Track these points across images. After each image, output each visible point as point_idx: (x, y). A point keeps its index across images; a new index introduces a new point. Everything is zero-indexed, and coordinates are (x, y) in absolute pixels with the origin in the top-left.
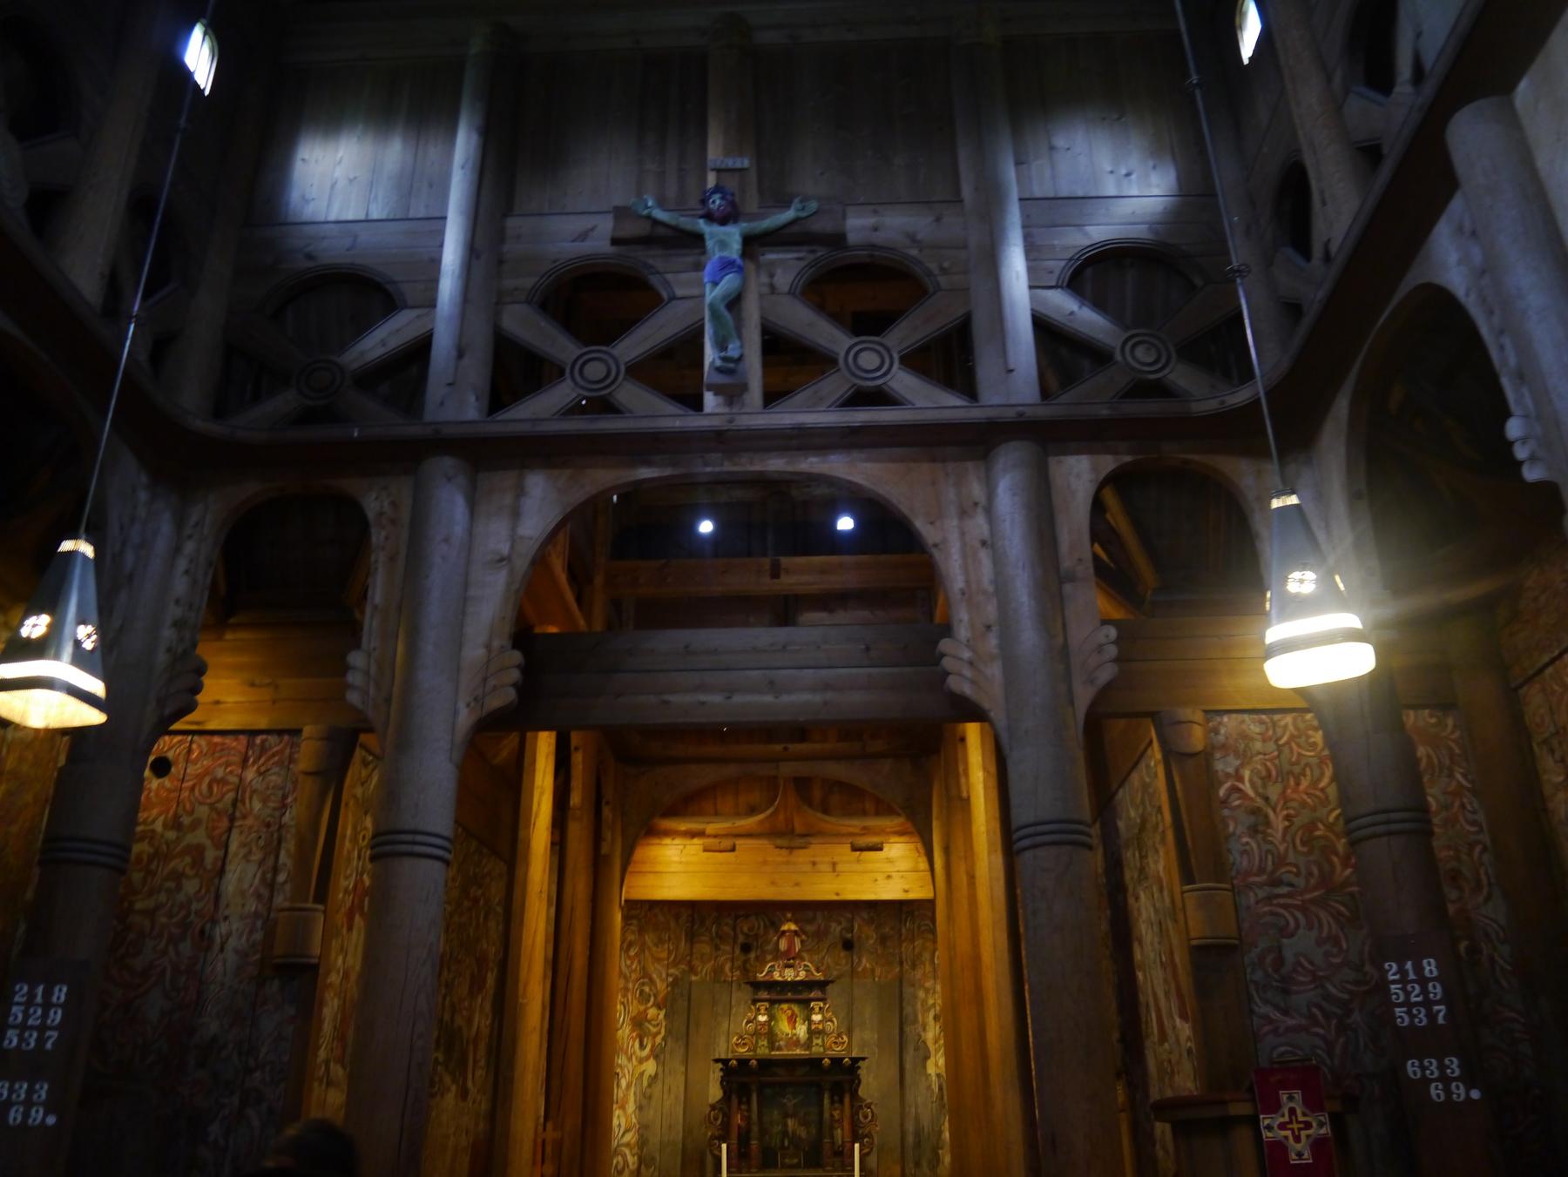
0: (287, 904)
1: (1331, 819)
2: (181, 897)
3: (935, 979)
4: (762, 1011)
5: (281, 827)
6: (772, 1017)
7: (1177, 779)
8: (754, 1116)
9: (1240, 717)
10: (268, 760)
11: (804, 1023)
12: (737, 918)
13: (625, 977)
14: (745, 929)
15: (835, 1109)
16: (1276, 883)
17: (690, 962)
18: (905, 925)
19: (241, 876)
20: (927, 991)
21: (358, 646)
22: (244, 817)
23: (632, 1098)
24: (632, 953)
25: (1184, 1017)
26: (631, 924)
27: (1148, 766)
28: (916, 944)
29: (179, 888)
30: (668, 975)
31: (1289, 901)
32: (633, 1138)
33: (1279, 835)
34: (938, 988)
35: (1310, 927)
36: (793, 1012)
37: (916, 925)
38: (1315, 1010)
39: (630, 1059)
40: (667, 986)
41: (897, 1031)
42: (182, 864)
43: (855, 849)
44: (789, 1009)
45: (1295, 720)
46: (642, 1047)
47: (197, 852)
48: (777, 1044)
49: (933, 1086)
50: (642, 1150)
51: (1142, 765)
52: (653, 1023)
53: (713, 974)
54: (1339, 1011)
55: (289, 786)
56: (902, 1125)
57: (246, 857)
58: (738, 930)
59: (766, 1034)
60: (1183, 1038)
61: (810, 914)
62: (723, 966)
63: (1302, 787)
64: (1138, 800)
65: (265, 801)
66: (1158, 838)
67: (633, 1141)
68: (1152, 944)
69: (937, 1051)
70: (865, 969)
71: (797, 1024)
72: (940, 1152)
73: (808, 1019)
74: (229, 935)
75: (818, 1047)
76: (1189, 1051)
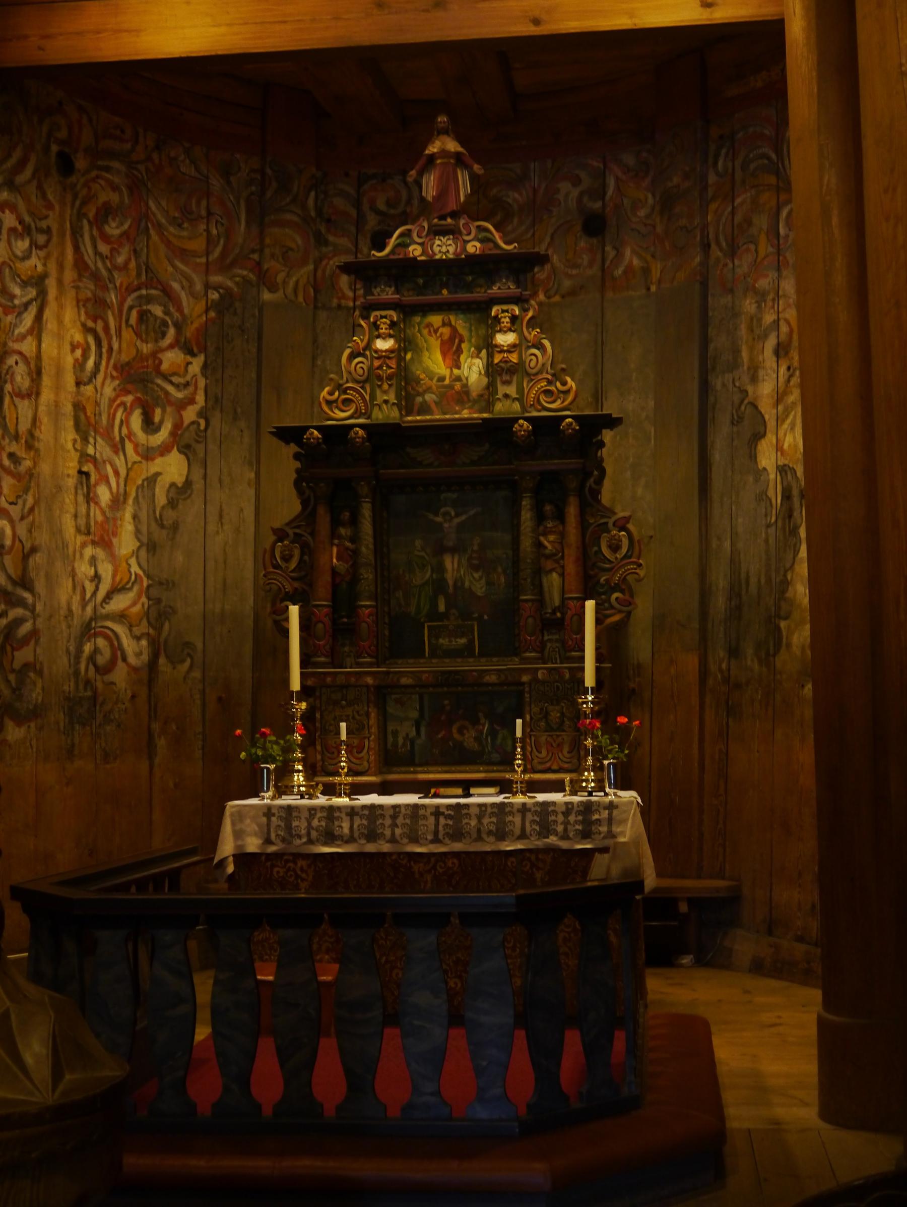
3: (779, 270)
4: (384, 330)
6: (406, 344)
11: (478, 357)
13: (96, 277)
14: (381, 206)
15: (545, 534)
17: (259, 264)
18: (715, 164)
20: (761, 296)
23: (128, 527)
24: (113, 229)
26: (108, 169)
28: (738, 201)
30: (207, 286)
32: (134, 604)
34: (788, 286)
36: (454, 330)
37: (738, 163)
39: (118, 447)
40: (207, 311)
41: (694, 387)
44: (444, 325)
46: (150, 425)
48: (419, 399)
49: (771, 493)
50: (159, 629)
52: (175, 379)
53: (312, 291)
56: (703, 575)
58: (366, 207)
59: (390, 378)
67: (137, 609)
69: (779, 420)
70: (629, 269)
71: (462, 358)
72: (783, 624)
75: (508, 402)
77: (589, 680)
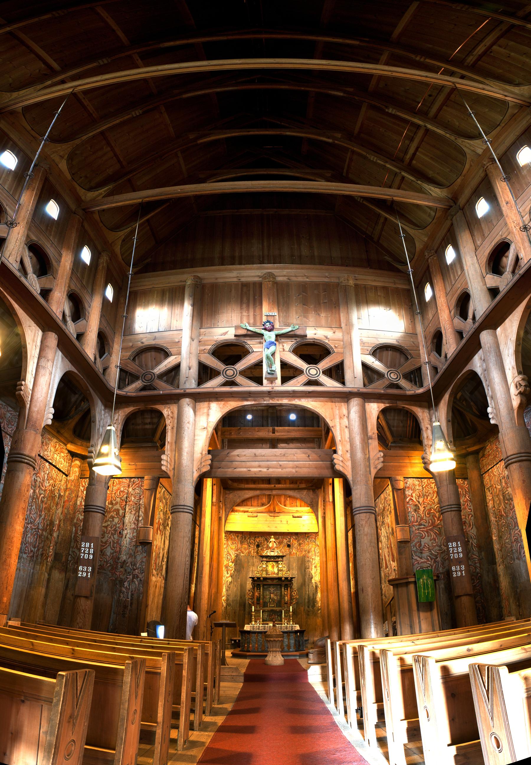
0: (142, 526)
1: (435, 508)
2: (114, 523)
5: (140, 504)
6: (267, 566)
7: (395, 496)
8: (261, 593)
9: (413, 479)
10: (135, 486)
12: (255, 537)
16: (421, 525)
19: (129, 518)
21: (164, 453)
22: (130, 502)
25: (393, 561)
27: (386, 493)
29: (113, 521)
31: (424, 530)
33: (422, 512)
35: (428, 536)
38: (428, 557)
42: (114, 514)
43: (294, 517)
45: (427, 481)
46: (227, 573)
47: (117, 511)
51: (385, 492)
54: (434, 558)
55: (141, 493)
57: (131, 513)
60: (393, 567)
61: (278, 536)
62: (251, 551)
63: (428, 499)
64: (383, 502)
65: (135, 497)
66: (388, 513)
68: (385, 542)
73: (278, 567)
74: (127, 534)
76: (395, 570)
77: (291, 611)
